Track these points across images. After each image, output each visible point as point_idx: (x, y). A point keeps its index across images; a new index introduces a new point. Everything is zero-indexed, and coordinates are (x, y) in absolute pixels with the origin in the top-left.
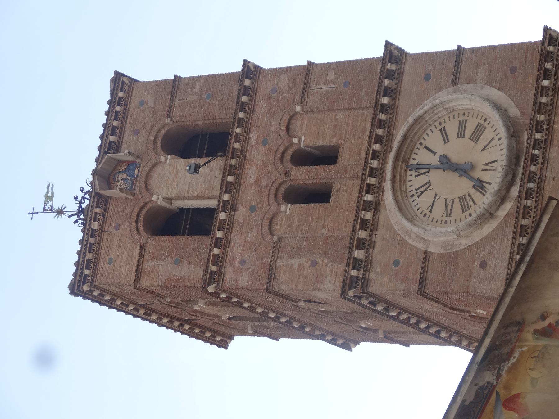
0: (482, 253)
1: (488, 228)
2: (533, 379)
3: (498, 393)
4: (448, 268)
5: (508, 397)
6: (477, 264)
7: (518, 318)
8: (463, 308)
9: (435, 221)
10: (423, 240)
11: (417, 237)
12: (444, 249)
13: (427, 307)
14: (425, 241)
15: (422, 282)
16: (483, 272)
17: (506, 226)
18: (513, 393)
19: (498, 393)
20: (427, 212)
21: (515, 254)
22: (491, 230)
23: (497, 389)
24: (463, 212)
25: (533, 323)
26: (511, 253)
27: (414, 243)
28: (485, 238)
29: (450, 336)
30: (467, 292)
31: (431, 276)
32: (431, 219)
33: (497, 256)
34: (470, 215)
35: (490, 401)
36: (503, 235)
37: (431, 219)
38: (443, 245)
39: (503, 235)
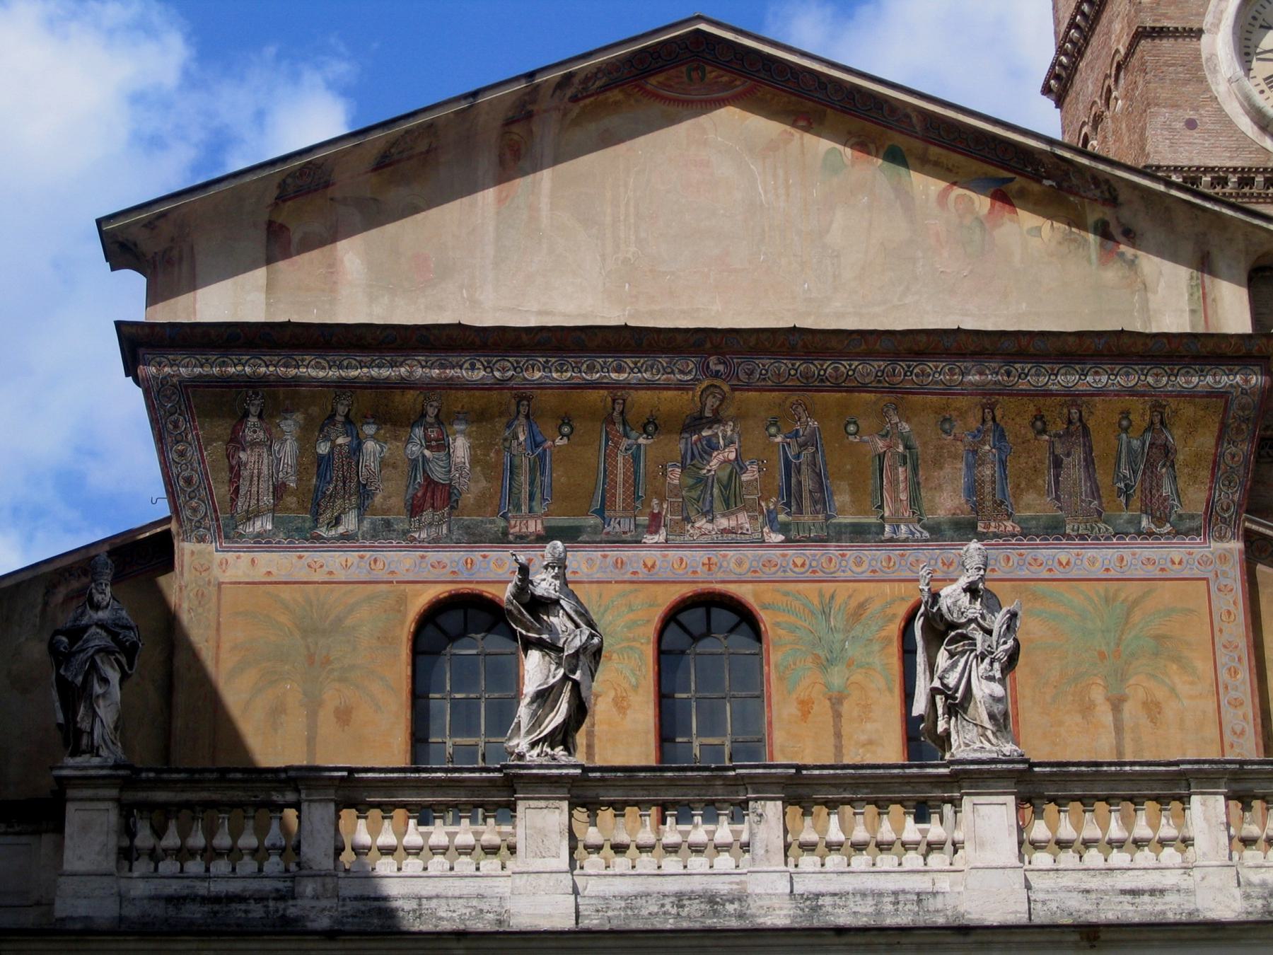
0: (1207, 120)
1: (1246, 124)
2: (1039, 229)
3: (1011, 180)
4: (1180, 69)
5: (1009, 195)
6: (1190, 114)
7: (1122, 198)
8: (1122, 82)
9: (1248, 35)
10: (1217, 22)
11: (1222, 12)
12: (1208, 60)
13: (1117, 27)
14: (1217, 25)
15: (1159, 33)
16: (1180, 125)
17: (1250, 152)
18: (1014, 201)
19: (1011, 180)
20: (1260, 22)
21: (1213, 175)
22: (1243, 128)
23: (1018, 178)
24: (1265, 80)
25: (1117, 218)
26: (1213, 169)
27: (1211, 7)
28: (1231, 122)
29: (1071, 41)
30: (1148, 104)
31: (1166, 44)
32: (1250, 28)
33: (1207, 144)
34: (1262, 92)
35: (1001, 171)
36: (1237, 149)
37: (1250, 28)
38: (1213, 56)
39: (1237, 149)
